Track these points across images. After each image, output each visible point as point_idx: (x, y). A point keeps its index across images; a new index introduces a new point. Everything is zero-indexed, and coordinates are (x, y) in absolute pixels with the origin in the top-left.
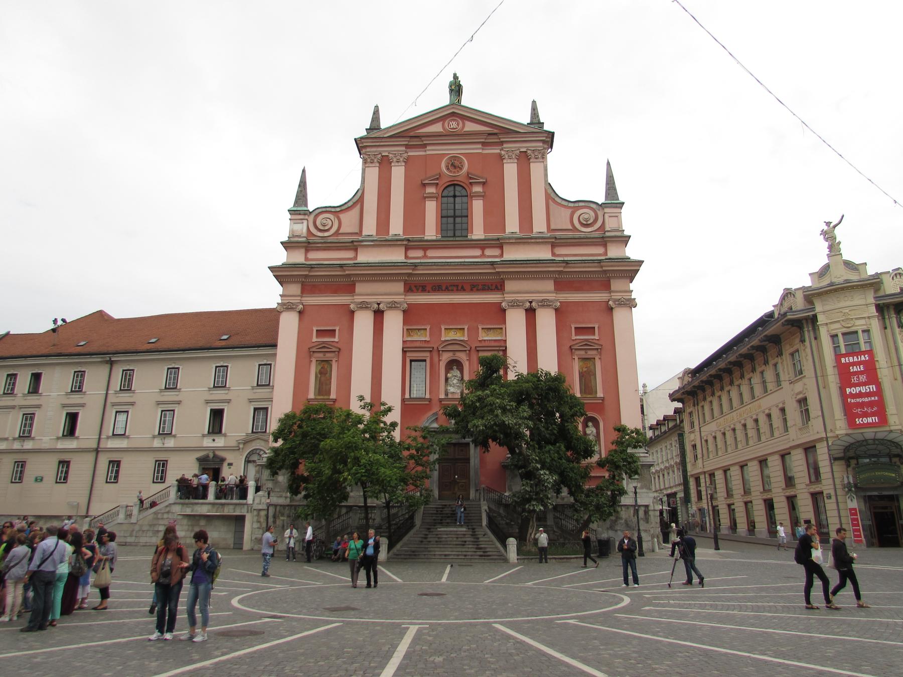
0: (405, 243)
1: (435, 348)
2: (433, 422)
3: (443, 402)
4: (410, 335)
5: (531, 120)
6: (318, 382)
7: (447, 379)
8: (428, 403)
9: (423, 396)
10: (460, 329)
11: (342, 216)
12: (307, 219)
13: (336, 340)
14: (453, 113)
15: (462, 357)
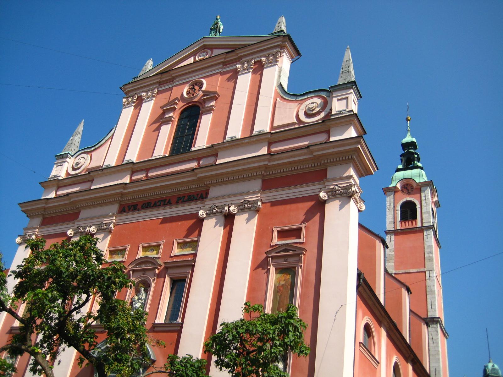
11: (93, 154)
14: (204, 45)
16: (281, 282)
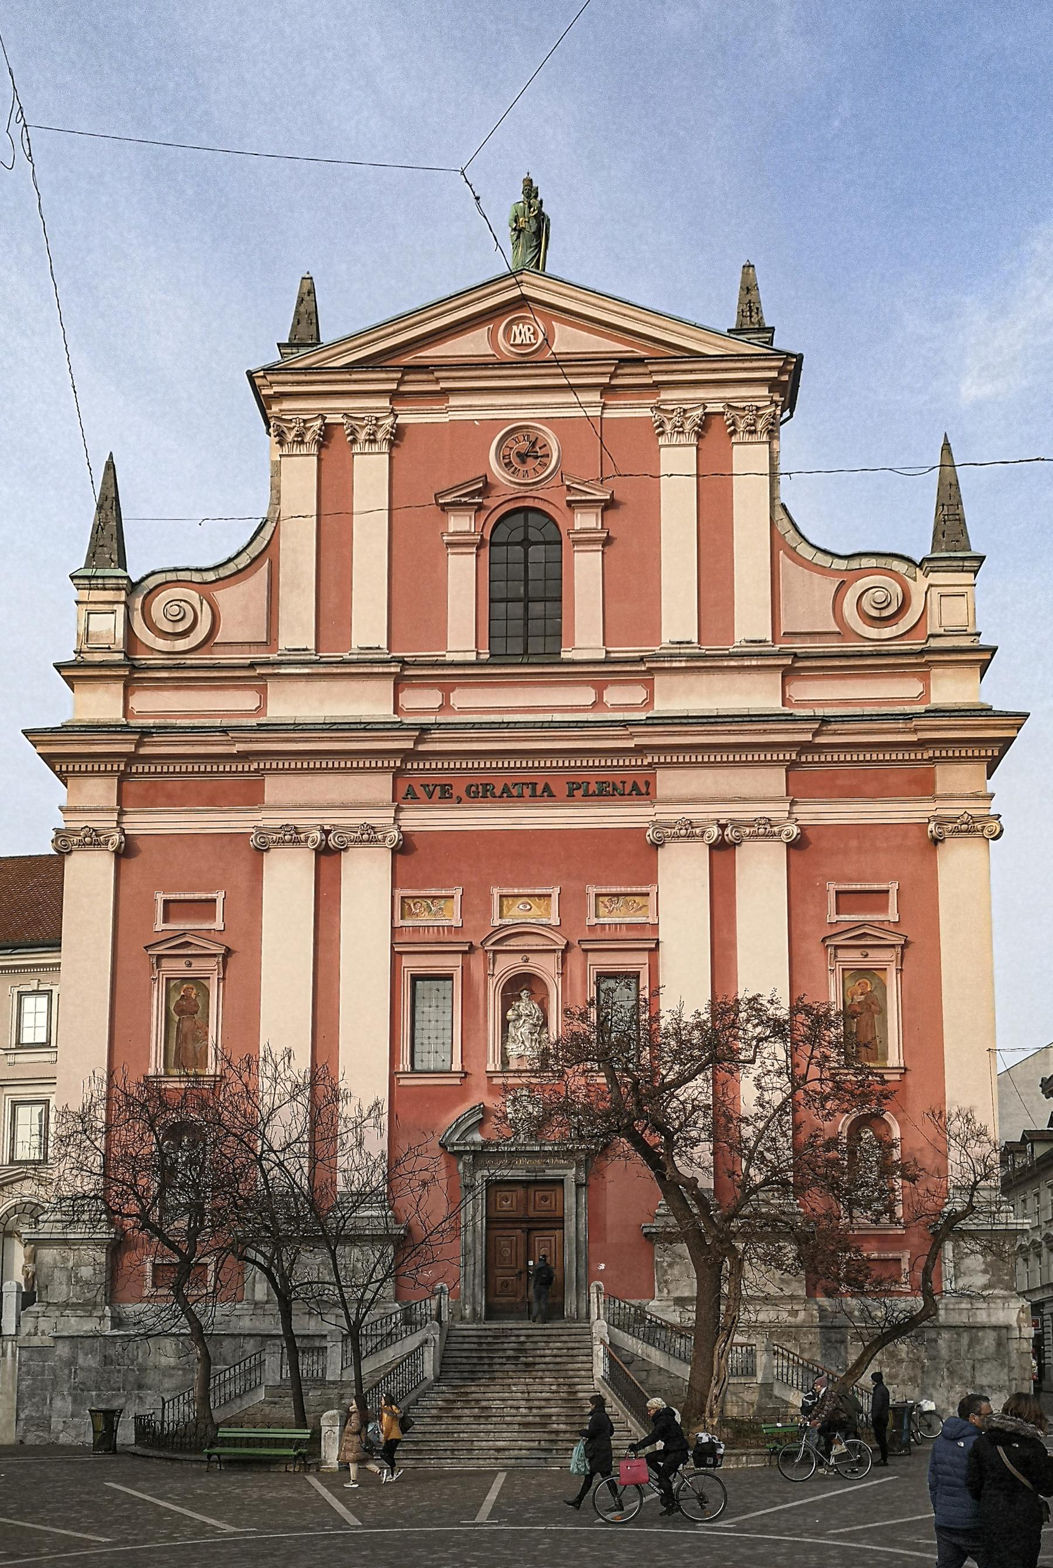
0: (393, 670)
1: (476, 943)
2: (470, 1130)
3: (495, 1081)
4: (411, 914)
5: (740, 323)
6: (174, 1033)
7: (505, 1024)
8: (457, 1081)
9: (447, 1067)
10: (539, 896)
12: (125, 603)
13: (218, 924)
14: (523, 298)
15: (546, 967)
16: (855, 997)
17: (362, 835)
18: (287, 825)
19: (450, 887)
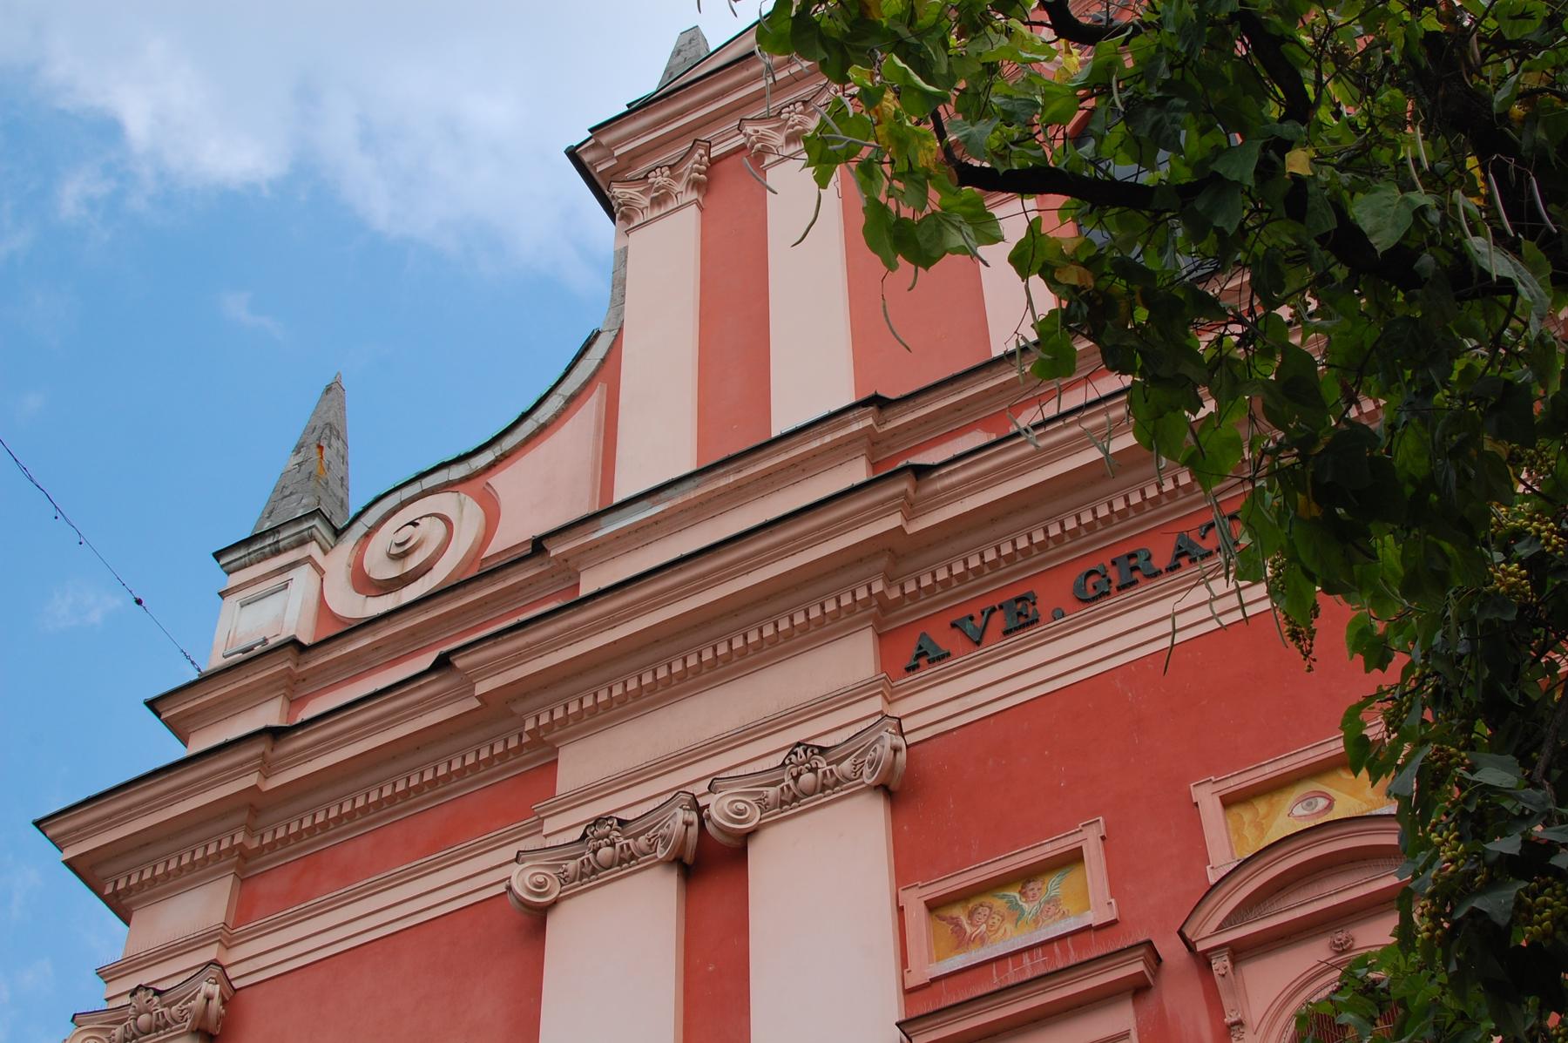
0: (855, 427)
1: (1170, 949)
4: (961, 941)
11: (500, 481)
17: (796, 778)
18: (598, 821)
19: (1066, 827)
